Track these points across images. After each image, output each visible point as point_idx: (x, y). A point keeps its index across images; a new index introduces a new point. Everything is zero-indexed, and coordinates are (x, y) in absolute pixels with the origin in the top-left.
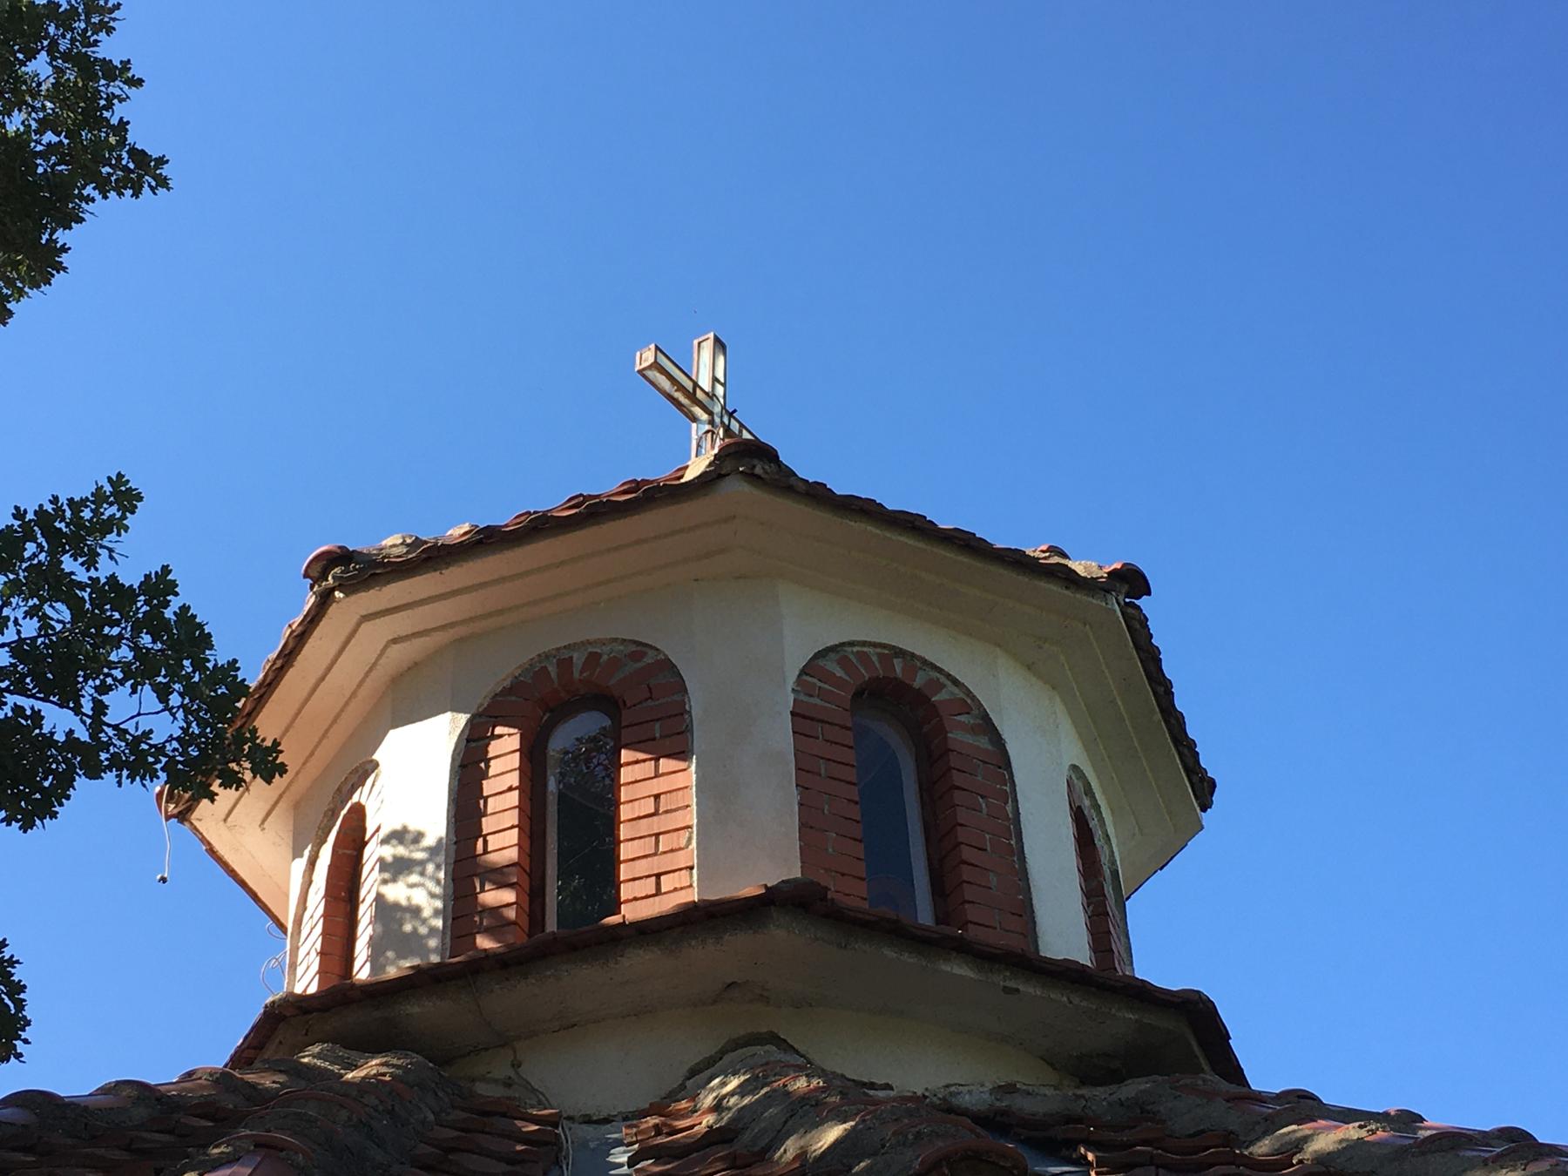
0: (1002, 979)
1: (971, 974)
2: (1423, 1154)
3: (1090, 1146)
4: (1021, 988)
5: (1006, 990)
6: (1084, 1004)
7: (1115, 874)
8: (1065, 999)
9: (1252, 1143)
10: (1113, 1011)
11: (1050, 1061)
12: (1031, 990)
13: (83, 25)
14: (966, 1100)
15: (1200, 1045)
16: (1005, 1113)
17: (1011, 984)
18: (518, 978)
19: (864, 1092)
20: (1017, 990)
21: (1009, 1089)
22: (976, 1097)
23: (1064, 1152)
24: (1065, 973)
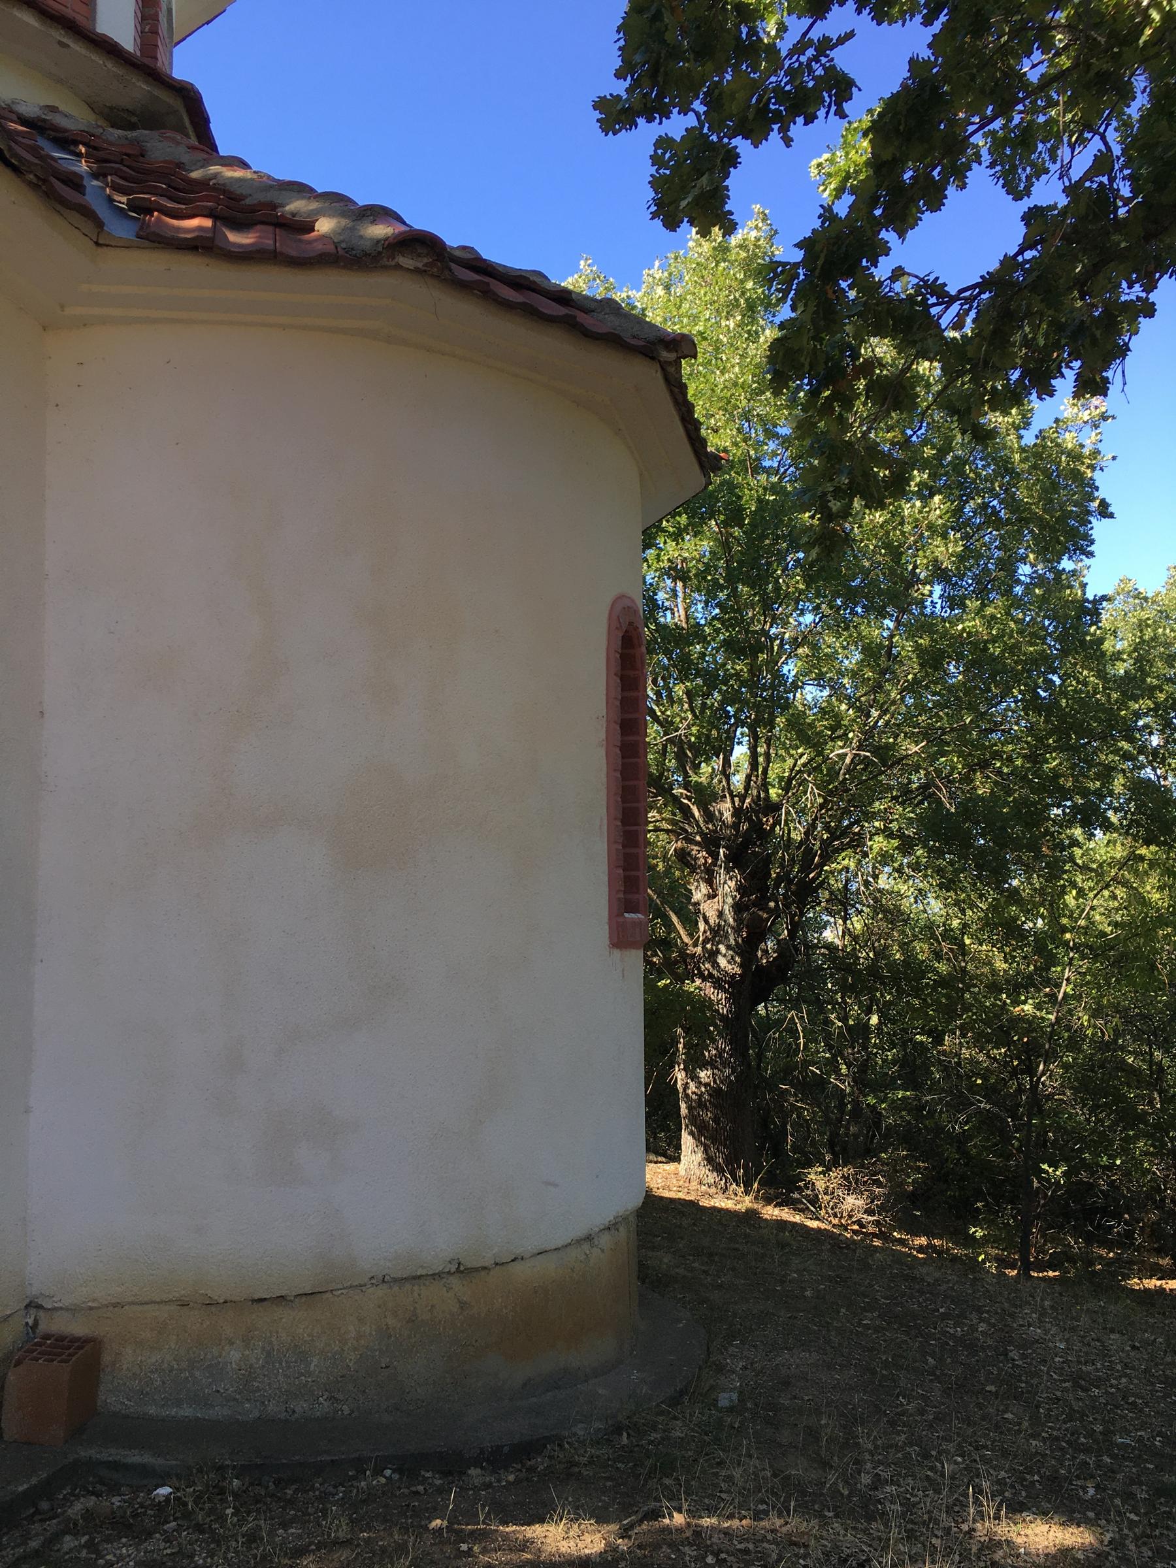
0: (58, 34)
1: (36, 24)
2: (280, 190)
3: (84, 144)
4: (72, 45)
5: (61, 44)
6: (115, 69)
7: (170, 11)
8: (101, 62)
9: (192, 171)
10: (134, 80)
11: (91, 106)
12: (78, 49)
13: (986, 538)
14: (23, 109)
15: (192, 122)
16: (44, 121)
17: (64, 40)
18: (738, 959)
19: (706, 822)
20: (68, 46)
21: (53, 109)
22: (29, 109)
23: (72, 148)
24: (109, 48)
